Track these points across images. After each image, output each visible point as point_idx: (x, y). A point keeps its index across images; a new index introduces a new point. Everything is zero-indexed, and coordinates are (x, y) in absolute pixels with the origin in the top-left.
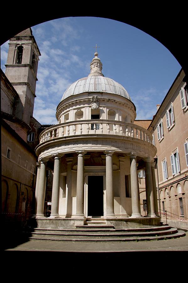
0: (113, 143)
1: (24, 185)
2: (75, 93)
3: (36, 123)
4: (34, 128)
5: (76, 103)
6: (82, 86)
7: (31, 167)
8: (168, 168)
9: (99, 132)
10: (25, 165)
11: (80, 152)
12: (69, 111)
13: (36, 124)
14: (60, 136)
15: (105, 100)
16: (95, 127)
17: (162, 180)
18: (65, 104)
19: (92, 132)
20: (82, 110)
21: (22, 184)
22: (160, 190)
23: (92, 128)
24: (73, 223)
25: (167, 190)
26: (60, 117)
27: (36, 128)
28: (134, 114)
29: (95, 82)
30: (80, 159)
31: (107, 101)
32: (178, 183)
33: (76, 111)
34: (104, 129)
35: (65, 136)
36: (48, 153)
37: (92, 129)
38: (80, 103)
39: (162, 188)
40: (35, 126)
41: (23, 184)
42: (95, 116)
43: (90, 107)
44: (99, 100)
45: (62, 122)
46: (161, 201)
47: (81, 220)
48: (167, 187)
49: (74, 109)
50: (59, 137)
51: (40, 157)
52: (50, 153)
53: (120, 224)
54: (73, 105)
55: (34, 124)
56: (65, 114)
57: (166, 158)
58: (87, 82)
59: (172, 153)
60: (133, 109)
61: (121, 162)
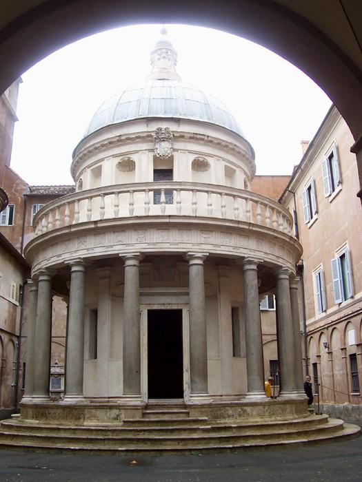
2: (115, 118)
3: (18, 181)
5: (120, 141)
8: (328, 287)
9: (171, 210)
11: (129, 255)
14: (83, 219)
16: (163, 198)
17: (313, 315)
18: (94, 144)
19: (155, 210)
20: (134, 157)
23: (155, 200)
25: (323, 336)
26: (81, 174)
28: (252, 167)
30: (131, 273)
31: (191, 138)
32: (347, 321)
33: (118, 160)
34: (184, 205)
35: (93, 219)
36: (55, 259)
37: (156, 201)
39: (313, 332)
42: (163, 173)
43: (152, 150)
45: (87, 187)
46: (311, 362)
49: (115, 156)
50: (80, 221)
51: (36, 268)
52: (60, 258)
54: (111, 144)
56: (91, 168)
57: (321, 264)
59: (336, 254)
61: (222, 279)
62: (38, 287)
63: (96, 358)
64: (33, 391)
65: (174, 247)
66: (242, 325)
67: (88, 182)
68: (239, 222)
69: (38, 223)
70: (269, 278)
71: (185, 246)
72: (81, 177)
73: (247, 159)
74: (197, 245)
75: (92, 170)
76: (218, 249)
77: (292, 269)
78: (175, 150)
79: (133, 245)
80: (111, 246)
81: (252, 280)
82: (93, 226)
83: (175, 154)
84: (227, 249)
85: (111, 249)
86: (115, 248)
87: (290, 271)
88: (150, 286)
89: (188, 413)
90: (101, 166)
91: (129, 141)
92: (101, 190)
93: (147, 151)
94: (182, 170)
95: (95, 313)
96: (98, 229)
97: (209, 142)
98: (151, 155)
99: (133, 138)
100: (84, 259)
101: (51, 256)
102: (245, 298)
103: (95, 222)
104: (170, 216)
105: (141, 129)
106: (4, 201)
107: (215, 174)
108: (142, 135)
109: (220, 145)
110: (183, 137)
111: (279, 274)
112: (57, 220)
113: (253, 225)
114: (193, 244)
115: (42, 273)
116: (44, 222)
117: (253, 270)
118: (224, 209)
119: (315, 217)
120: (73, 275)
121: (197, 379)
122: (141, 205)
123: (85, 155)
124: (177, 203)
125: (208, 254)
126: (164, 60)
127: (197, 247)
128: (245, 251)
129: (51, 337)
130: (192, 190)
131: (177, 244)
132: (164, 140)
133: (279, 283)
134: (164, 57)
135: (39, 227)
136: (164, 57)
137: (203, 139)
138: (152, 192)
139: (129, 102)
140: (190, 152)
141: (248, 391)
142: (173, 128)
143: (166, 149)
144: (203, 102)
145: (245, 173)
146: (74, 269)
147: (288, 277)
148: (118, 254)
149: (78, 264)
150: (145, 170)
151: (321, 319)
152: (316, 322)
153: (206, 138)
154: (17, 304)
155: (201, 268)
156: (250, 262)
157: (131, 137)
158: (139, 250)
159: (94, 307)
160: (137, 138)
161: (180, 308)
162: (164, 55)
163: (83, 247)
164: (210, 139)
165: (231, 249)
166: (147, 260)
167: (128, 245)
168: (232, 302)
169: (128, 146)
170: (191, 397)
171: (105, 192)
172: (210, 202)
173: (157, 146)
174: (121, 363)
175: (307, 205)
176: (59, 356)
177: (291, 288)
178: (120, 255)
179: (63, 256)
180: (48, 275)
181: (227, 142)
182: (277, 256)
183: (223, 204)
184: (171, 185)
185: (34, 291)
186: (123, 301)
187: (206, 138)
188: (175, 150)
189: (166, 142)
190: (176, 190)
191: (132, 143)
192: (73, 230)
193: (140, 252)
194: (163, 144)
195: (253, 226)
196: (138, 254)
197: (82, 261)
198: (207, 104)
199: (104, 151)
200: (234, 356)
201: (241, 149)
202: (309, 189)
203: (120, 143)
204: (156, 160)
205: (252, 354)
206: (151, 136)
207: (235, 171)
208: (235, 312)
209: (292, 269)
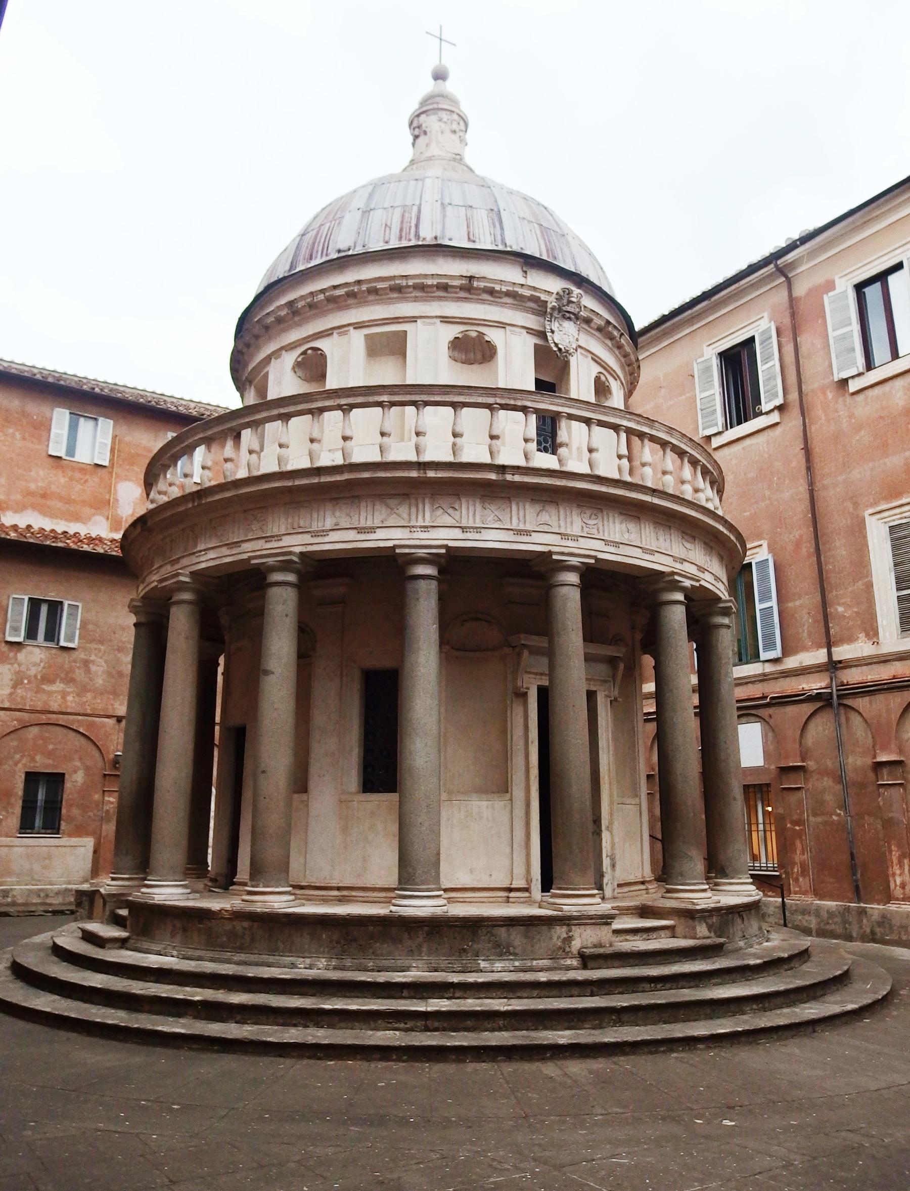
11: (574, 561)
38: (492, 294)
79: (576, 538)
108: (521, 291)
126: (453, 136)
134: (454, 132)
148: (550, 553)
160: (508, 294)
167: (564, 536)
171: (420, 396)
189: (572, 323)
191: (491, 303)
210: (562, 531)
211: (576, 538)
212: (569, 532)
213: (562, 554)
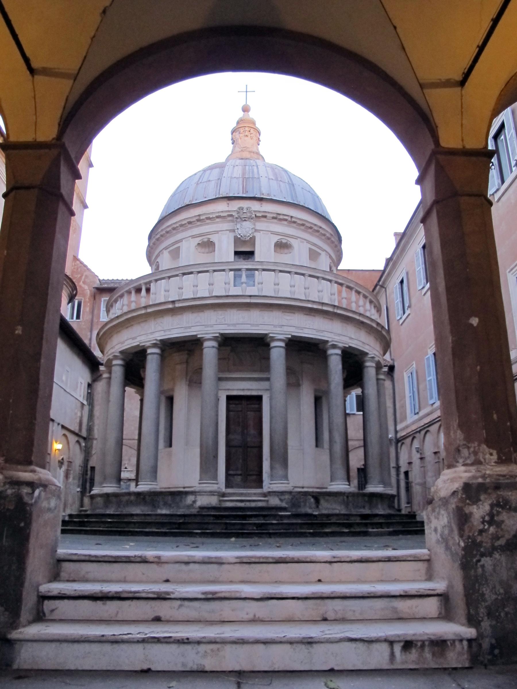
0: (288, 318)
1: (60, 427)
3: (87, 273)
4: (83, 286)
5: (200, 220)
6: (213, 182)
7: (77, 383)
8: (421, 387)
10: (64, 378)
12: (181, 241)
13: (86, 276)
15: (268, 218)
16: (244, 278)
17: (404, 418)
20: (214, 238)
21: (56, 424)
22: (399, 444)
24: (193, 499)
27: (86, 287)
29: (244, 174)
31: (274, 218)
33: (198, 240)
34: (266, 285)
36: (130, 341)
39: (405, 438)
40: (84, 283)
41: (59, 424)
43: (234, 231)
44: (254, 216)
46: (403, 470)
47: (212, 493)
48: (417, 435)
49: (193, 237)
51: (110, 352)
53: (302, 504)
55: (81, 277)
56: (168, 250)
57: (414, 363)
58: (225, 174)
60: (334, 239)
62: (110, 373)
63: (171, 446)
64: (105, 479)
65: (254, 328)
66: (325, 416)
67: (166, 262)
68: (323, 304)
69: (112, 306)
70: (354, 365)
71: (266, 327)
72: (158, 260)
73: (333, 242)
74: (280, 327)
75: (169, 252)
76: (301, 331)
77: (379, 357)
78: (256, 231)
80: (190, 327)
81: (335, 364)
82: (170, 306)
83: (258, 235)
84: (310, 331)
85: (189, 330)
86: (193, 329)
87: (377, 359)
88: (229, 371)
89: (267, 501)
90: (179, 248)
91: (208, 221)
92: (179, 270)
93: (228, 232)
94: (264, 251)
95: (170, 400)
96: (174, 310)
97: (292, 222)
98: (232, 236)
99: (213, 218)
100: (161, 340)
101: (125, 339)
102: (328, 383)
103: (173, 302)
104: (250, 296)
105: (222, 207)
106: (73, 292)
107: (299, 255)
108: (222, 214)
109: (303, 225)
110: (265, 217)
111: (364, 362)
112: (132, 302)
113: (338, 307)
114: (275, 326)
115: (116, 357)
116: (118, 305)
117: (337, 354)
118: (307, 291)
119: (407, 312)
120: (149, 357)
121: (277, 466)
122: (222, 285)
123: (162, 236)
124: (258, 284)
125: (290, 336)
126: (246, 138)
127: (278, 329)
128: (329, 335)
129: (122, 439)
130: (274, 270)
131: (257, 325)
132: (245, 220)
133: (365, 370)
134: (247, 136)
135: (112, 311)
136: (247, 136)
137: (286, 220)
138: (233, 272)
139: (209, 181)
140: (273, 233)
141: (332, 481)
142: (255, 206)
143: (247, 230)
144: (287, 181)
145: (330, 257)
146: (149, 351)
147: (374, 365)
148: (196, 335)
149: (155, 345)
150: (225, 251)
151: (413, 423)
152: (407, 427)
153: (289, 219)
154: (85, 402)
155: (283, 351)
156: (334, 346)
157: (211, 216)
158: (219, 331)
159: (170, 394)
160: (218, 217)
161: (260, 393)
162: (247, 133)
163: (160, 328)
164: (293, 220)
165: (314, 332)
166: (229, 343)
168: (316, 391)
169: (207, 227)
170: (271, 484)
172: (293, 284)
173: (238, 226)
174: (198, 450)
175: (399, 299)
176: (129, 460)
177: (378, 379)
178: (198, 336)
179: (139, 339)
180: (123, 359)
181: (312, 223)
182: (363, 343)
183: (307, 286)
184: (253, 265)
185: (106, 378)
186: (200, 387)
187: (289, 219)
188: (256, 231)
190: (257, 270)
192: (149, 310)
193: (219, 333)
194: (244, 223)
195: (337, 309)
196: (218, 335)
197: (158, 342)
198: (292, 185)
199: (183, 231)
200: (317, 446)
201: (327, 231)
202: (402, 282)
203: (199, 223)
204: (237, 241)
205: (335, 442)
206: (231, 216)
207: (320, 254)
208: (318, 400)
209: (379, 357)
210: (206, 324)
211: (211, 326)
212: (209, 324)
213: (202, 334)
